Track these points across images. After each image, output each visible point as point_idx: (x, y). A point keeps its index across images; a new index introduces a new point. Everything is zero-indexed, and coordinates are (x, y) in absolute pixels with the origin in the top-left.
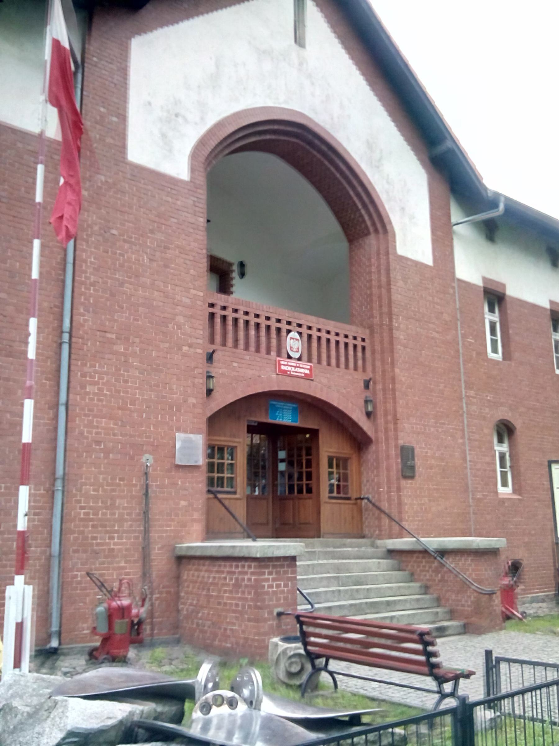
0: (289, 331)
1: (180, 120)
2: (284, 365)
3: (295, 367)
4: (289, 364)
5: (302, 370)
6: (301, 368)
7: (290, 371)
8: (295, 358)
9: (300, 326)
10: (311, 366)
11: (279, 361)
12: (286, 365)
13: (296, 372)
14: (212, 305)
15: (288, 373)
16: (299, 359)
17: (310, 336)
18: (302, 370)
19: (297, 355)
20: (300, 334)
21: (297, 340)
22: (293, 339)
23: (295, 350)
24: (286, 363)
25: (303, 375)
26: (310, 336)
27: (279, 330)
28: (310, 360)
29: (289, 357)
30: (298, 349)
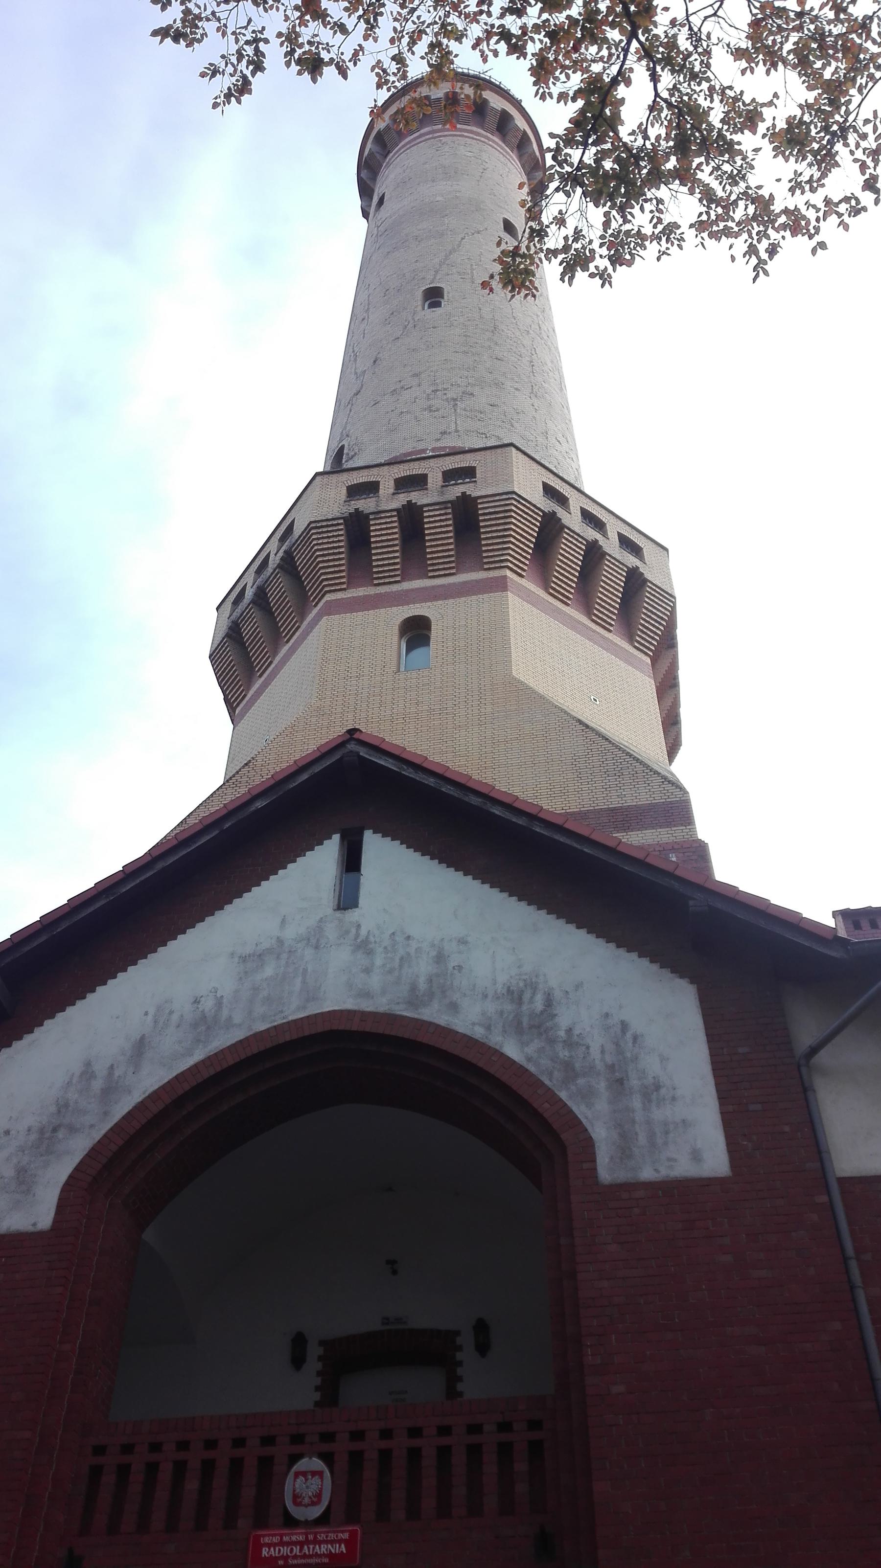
0: (294, 1459)
1: (60, 1135)
2: (269, 1545)
3: (301, 1544)
4: (286, 1539)
5: (323, 1549)
6: (320, 1543)
7: (285, 1558)
8: (306, 1522)
9: (328, 1437)
10: (353, 1534)
11: (257, 1538)
12: (274, 1545)
13: (305, 1556)
14: (99, 1450)
15: (281, 1562)
16: (323, 1520)
17: (356, 1458)
18: (323, 1549)
19: (316, 1512)
20: (328, 1458)
21: (320, 1474)
22: (304, 1474)
23: (307, 1501)
24: (276, 1540)
25: (326, 1560)
26: (356, 1458)
27: (266, 1463)
28: (352, 1515)
29: (290, 1522)
30: (319, 1496)
